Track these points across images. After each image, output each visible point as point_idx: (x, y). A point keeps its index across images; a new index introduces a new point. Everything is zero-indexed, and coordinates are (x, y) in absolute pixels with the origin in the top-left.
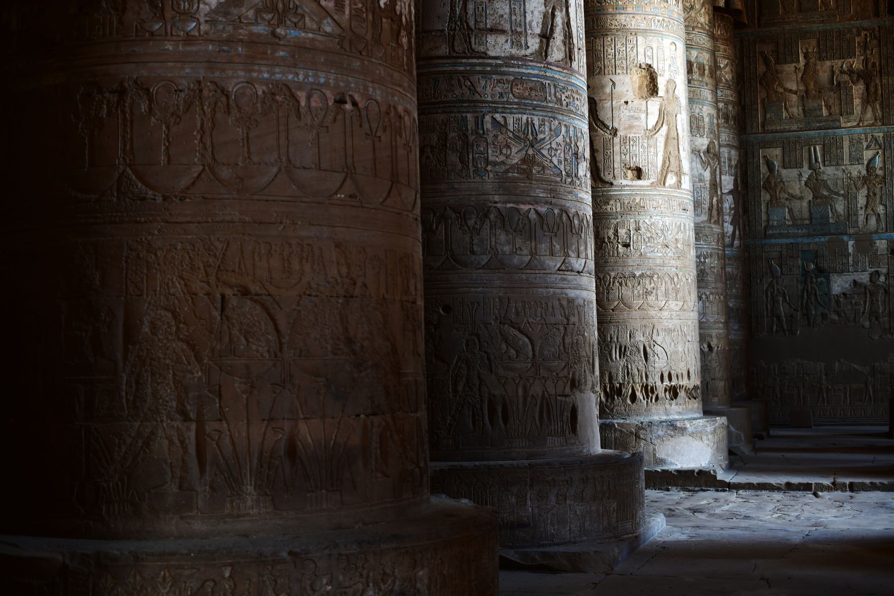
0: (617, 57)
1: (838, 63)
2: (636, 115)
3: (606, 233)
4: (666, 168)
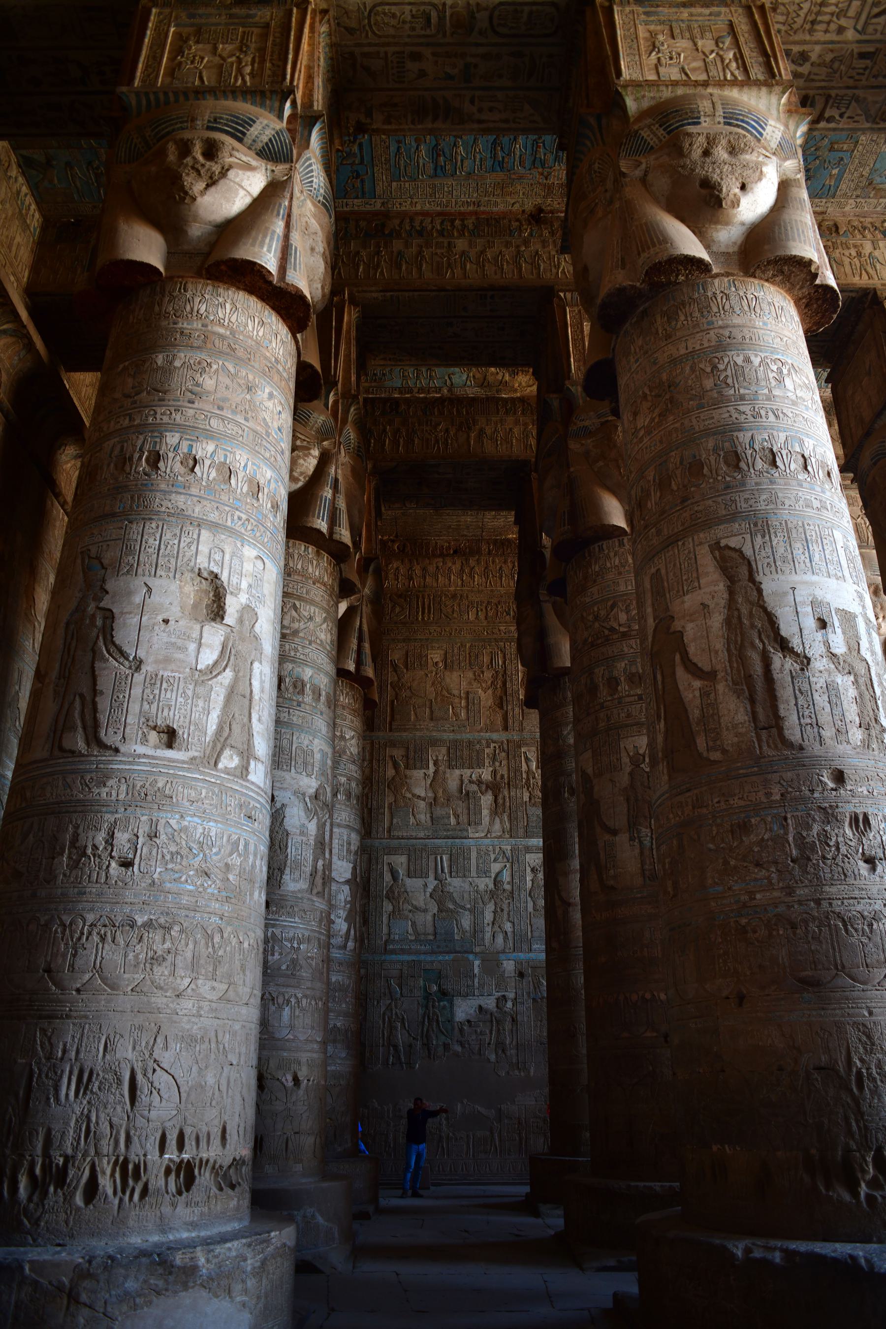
0: (161, 552)
1: (467, 772)
2: (179, 642)
3: (90, 839)
4: (222, 740)
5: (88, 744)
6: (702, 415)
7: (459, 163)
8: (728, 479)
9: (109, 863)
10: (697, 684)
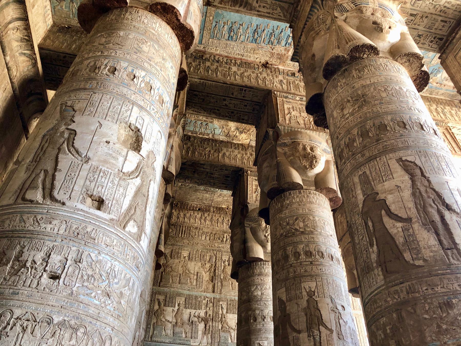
0: (110, 109)
1: (193, 311)
2: (114, 155)
4: (130, 215)
5: (44, 198)
6: (383, 107)
7: (239, 37)
8: (401, 132)
9: (42, 275)
10: (399, 225)
